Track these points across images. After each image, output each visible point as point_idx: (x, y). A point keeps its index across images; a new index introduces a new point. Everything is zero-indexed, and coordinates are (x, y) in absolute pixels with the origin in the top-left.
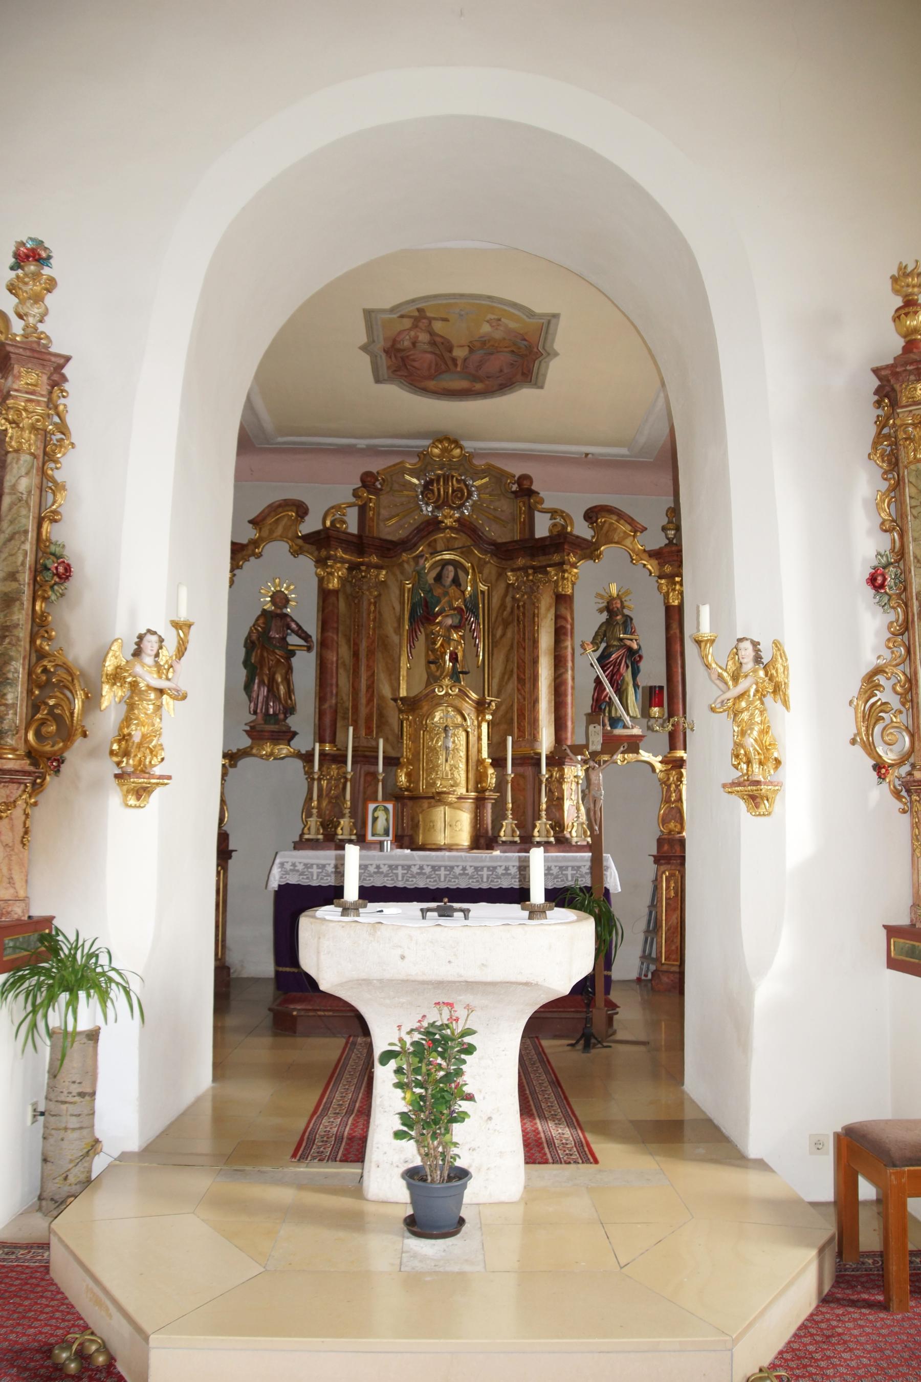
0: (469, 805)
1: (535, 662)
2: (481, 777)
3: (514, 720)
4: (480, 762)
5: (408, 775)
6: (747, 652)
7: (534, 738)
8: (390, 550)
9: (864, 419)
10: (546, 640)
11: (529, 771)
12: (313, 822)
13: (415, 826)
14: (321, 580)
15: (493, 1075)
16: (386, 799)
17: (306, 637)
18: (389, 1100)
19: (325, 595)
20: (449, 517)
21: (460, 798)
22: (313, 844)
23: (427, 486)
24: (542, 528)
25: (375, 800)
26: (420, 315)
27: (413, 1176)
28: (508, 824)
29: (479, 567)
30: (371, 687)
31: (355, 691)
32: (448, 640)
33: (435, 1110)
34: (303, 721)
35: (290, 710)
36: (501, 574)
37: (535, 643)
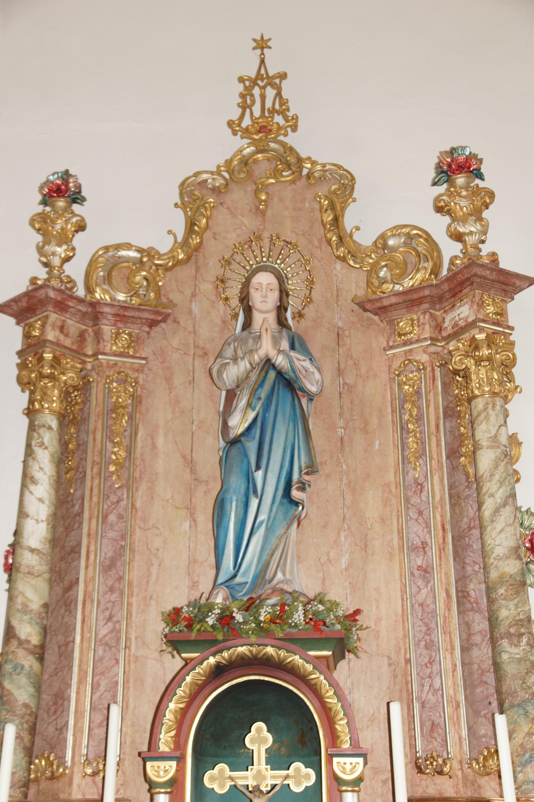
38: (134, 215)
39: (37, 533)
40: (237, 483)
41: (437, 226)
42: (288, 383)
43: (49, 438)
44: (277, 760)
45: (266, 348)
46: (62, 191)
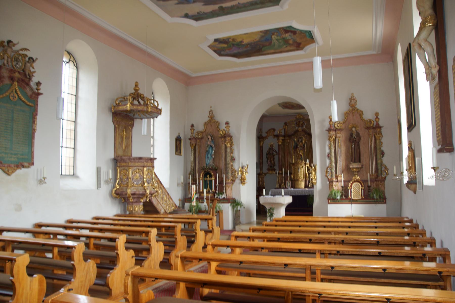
0: (304, 180)
4: (306, 173)
5: (294, 176)
17: (277, 152)
19: (279, 145)
20: (300, 129)
21: (302, 180)
22: (278, 188)
23: (296, 123)
25: (287, 180)
26: (286, 103)
29: (306, 138)
31: (285, 161)
32: (300, 152)
34: (276, 167)
35: (274, 165)
38: (200, 127)
41: (225, 129)
42: (211, 146)
45: (209, 143)
46: (192, 126)
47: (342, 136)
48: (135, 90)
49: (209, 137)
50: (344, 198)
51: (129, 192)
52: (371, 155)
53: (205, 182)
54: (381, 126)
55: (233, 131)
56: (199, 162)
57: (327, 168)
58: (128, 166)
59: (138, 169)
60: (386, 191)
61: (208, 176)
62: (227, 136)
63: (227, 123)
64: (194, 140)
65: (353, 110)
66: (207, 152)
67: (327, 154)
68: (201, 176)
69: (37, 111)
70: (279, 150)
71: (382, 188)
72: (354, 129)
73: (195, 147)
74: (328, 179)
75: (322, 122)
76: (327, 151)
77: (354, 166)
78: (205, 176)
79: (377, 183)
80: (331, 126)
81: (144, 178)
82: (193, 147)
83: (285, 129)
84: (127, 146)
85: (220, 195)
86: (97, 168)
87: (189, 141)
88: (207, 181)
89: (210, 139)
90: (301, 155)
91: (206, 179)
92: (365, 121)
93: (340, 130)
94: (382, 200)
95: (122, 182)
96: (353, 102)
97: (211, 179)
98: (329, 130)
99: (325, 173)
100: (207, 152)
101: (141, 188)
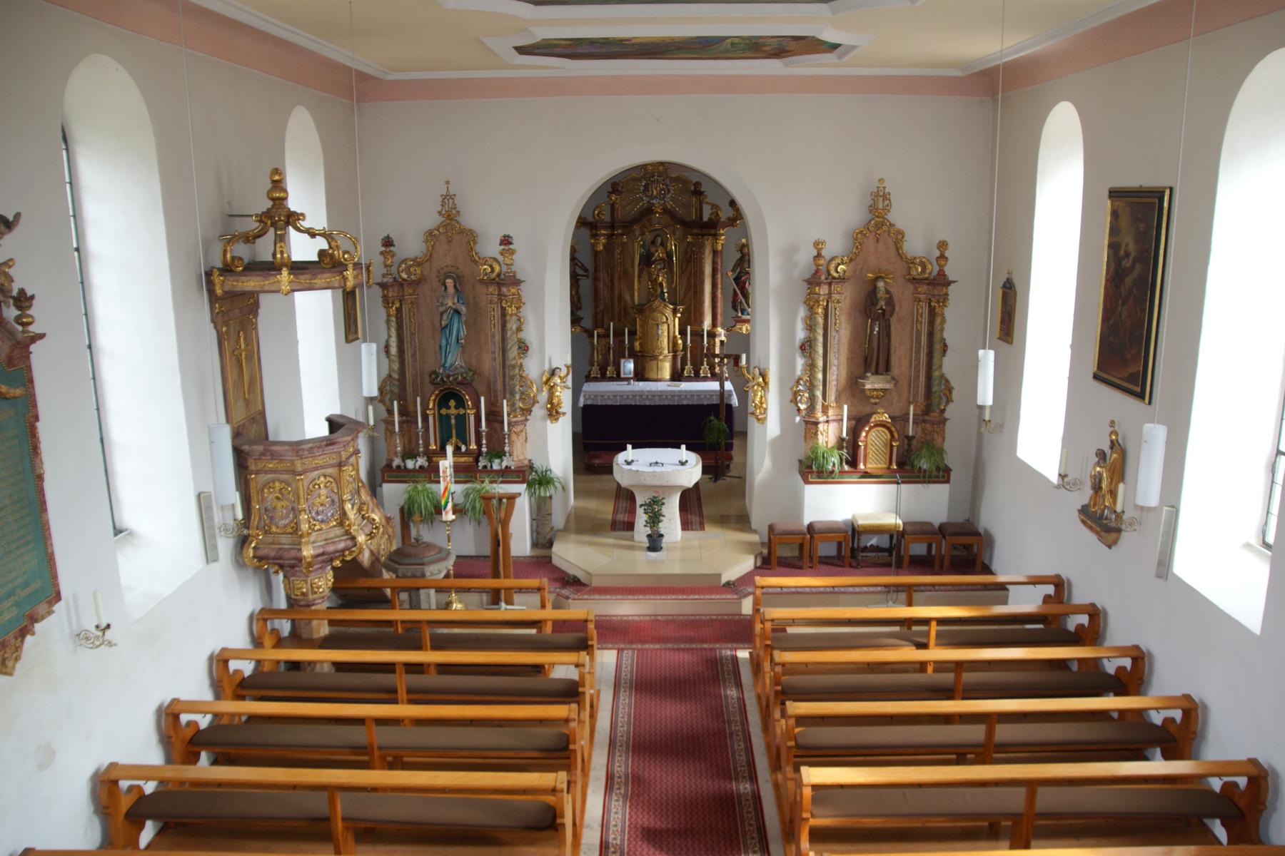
1: (702, 283)
2: (675, 344)
3: (691, 317)
4: (675, 337)
6: (757, 371)
7: (702, 322)
8: (628, 226)
9: (803, 289)
10: (708, 270)
11: (699, 339)
12: (595, 368)
13: (644, 369)
14: (593, 246)
15: (672, 509)
16: (630, 357)
17: (586, 270)
18: (641, 518)
19: (596, 254)
22: (596, 380)
23: (646, 186)
24: (705, 218)
25: (624, 357)
27: (649, 536)
28: (688, 367)
30: (620, 297)
33: (655, 519)
36: (685, 237)
37: (702, 273)
38: (411, 246)
39: (394, 350)
40: (444, 341)
41: (500, 258)
42: (457, 312)
43: (394, 324)
44: (456, 407)
45: (450, 304)
46: (388, 242)
47: (845, 298)
48: (273, 199)
49: (449, 282)
50: (846, 468)
51: (308, 552)
52: (918, 352)
53: (444, 420)
54: (951, 279)
55: (522, 263)
56: (414, 355)
57: (798, 382)
58: (294, 473)
59: (325, 476)
60: (946, 446)
61: (452, 403)
62: (505, 283)
63: (506, 241)
64: (396, 289)
65: (879, 226)
66: (443, 329)
67: (798, 344)
68: (431, 406)
69: (35, 406)
70: (596, 268)
71: (939, 441)
72: (881, 284)
73: (399, 310)
74: (799, 410)
75: (790, 252)
76: (801, 334)
77: (872, 383)
78: (443, 401)
79: (928, 426)
80: (817, 271)
81: (342, 502)
82: (393, 311)
83: (613, 206)
84: (252, 384)
85: (497, 461)
86: (199, 496)
87: (378, 291)
88: (448, 417)
89: (451, 289)
90: (661, 285)
91: (444, 411)
92: (911, 262)
93: (842, 280)
94: (941, 474)
95: (271, 519)
96: (881, 206)
97: (462, 411)
98: (813, 282)
99: (789, 396)
100: (443, 329)
101: (339, 531)
